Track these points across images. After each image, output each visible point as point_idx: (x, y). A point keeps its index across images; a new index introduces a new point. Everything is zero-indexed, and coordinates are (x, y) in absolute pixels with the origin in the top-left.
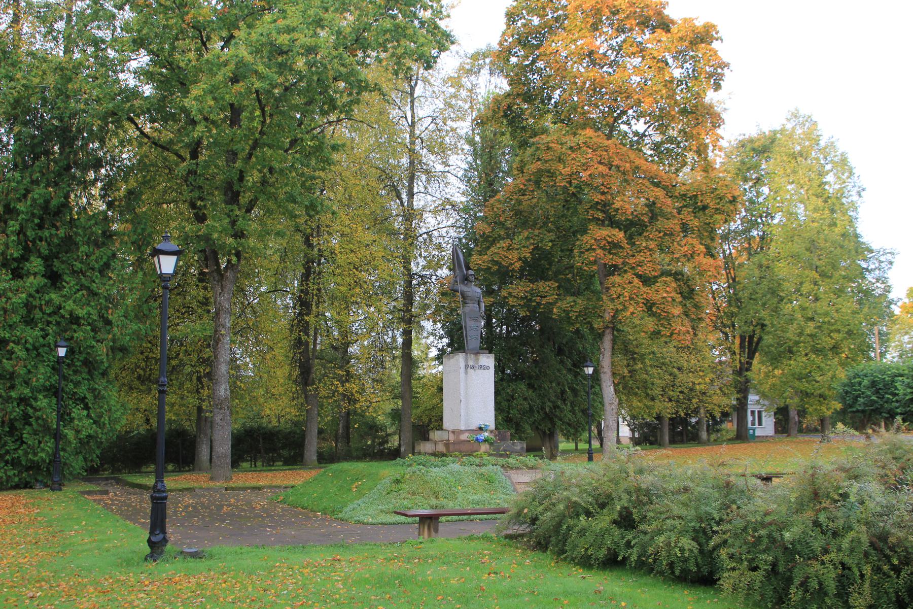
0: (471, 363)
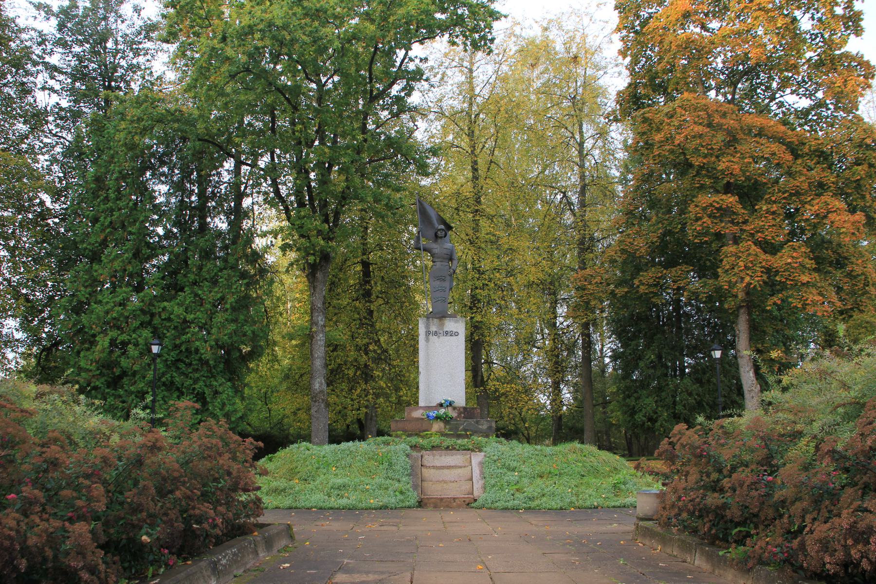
0: (433, 329)
